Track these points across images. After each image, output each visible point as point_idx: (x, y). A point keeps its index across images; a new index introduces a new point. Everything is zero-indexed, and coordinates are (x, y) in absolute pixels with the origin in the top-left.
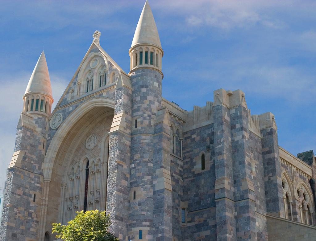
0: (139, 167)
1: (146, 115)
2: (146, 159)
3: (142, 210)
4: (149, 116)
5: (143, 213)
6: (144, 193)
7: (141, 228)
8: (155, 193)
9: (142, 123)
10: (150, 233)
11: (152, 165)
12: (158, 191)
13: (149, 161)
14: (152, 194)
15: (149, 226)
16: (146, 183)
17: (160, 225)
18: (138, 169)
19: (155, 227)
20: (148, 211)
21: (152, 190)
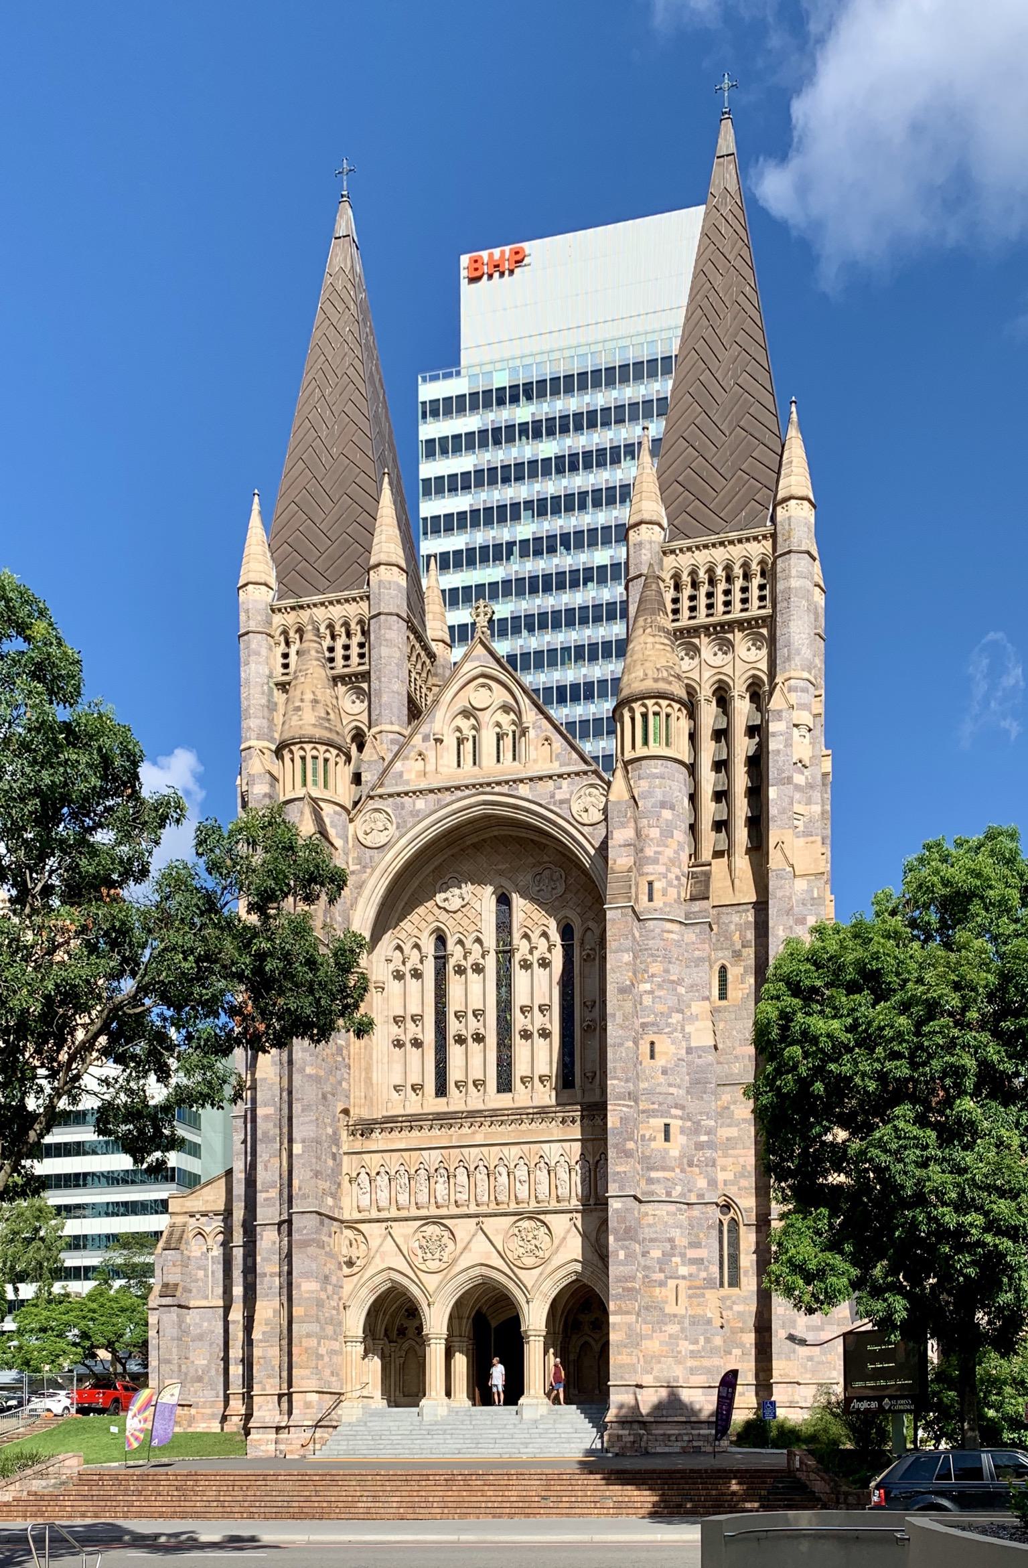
3: (670, 1085)
5: (672, 1090)
7: (667, 1121)
8: (689, 1050)
10: (682, 1132)
14: (684, 1052)
16: (676, 1030)
19: (690, 1120)
20: (679, 1087)
21: (684, 1044)
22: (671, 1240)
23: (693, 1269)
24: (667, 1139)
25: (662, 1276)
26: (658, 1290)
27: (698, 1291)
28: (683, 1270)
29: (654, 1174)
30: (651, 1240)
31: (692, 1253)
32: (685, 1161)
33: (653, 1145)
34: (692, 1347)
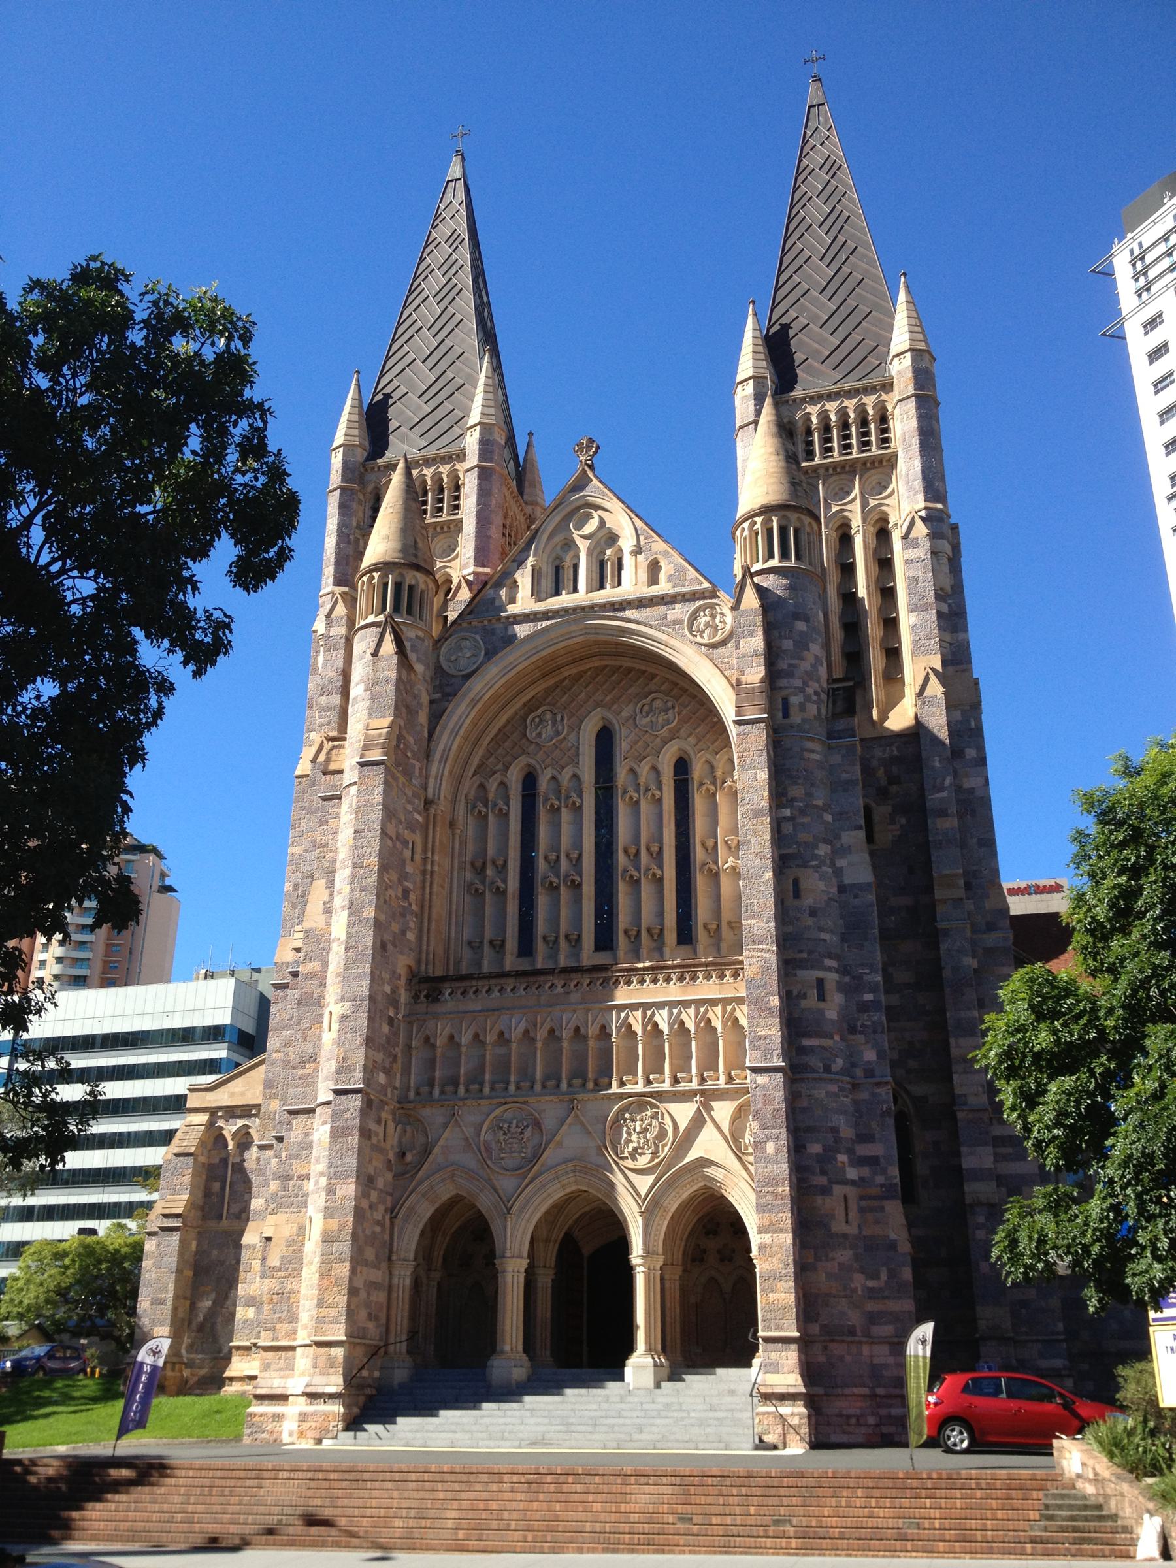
0: (805, 820)
1: (810, 691)
2: (820, 803)
3: (821, 929)
4: (816, 693)
6: (822, 885)
7: (821, 974)
8: (842, 889)
9: (802, 708)
11: (828, 818)
12: (853, 886)
13: (826, 808)
14: (834, 890)
15: (837, 971)
16: (823, 863)
17: (867, 971)
18: (803, 824)
20: (832, 932)
22: (835, 1130)
23: (866, 1171)
24: (822, 997)
25: (822, 1180)
26: (819, 1200)
27: (876, 1203)
28: (852, 1174)
29: (807, 1042)
30: (809, 1130)
31: (863, 1150)
32: (845, 1026)
33: (804, 1004)
34: (871, 1284)
